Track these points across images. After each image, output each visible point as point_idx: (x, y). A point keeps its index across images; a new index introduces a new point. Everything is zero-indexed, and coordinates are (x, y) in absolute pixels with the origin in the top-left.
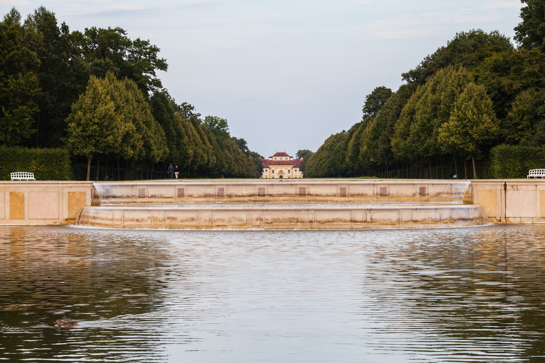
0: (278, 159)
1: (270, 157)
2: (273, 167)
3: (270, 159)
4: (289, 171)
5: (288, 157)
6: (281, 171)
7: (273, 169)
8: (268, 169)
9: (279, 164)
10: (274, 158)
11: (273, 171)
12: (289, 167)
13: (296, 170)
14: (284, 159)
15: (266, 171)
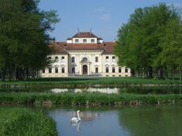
0: (81, 41)
1: (69, 39)
2: (73, 54)
3: (69, 42)
4: (97, 58)
5: (96, 39)
6: (85, 59)
7: (72, 56)
8: (66, 57)
9: (85, 49)
10: (74, 39)
11: (73, 58)
12: (98, 54)
13: (107, 58)
14: (89, 41)
15: (63, 58)
